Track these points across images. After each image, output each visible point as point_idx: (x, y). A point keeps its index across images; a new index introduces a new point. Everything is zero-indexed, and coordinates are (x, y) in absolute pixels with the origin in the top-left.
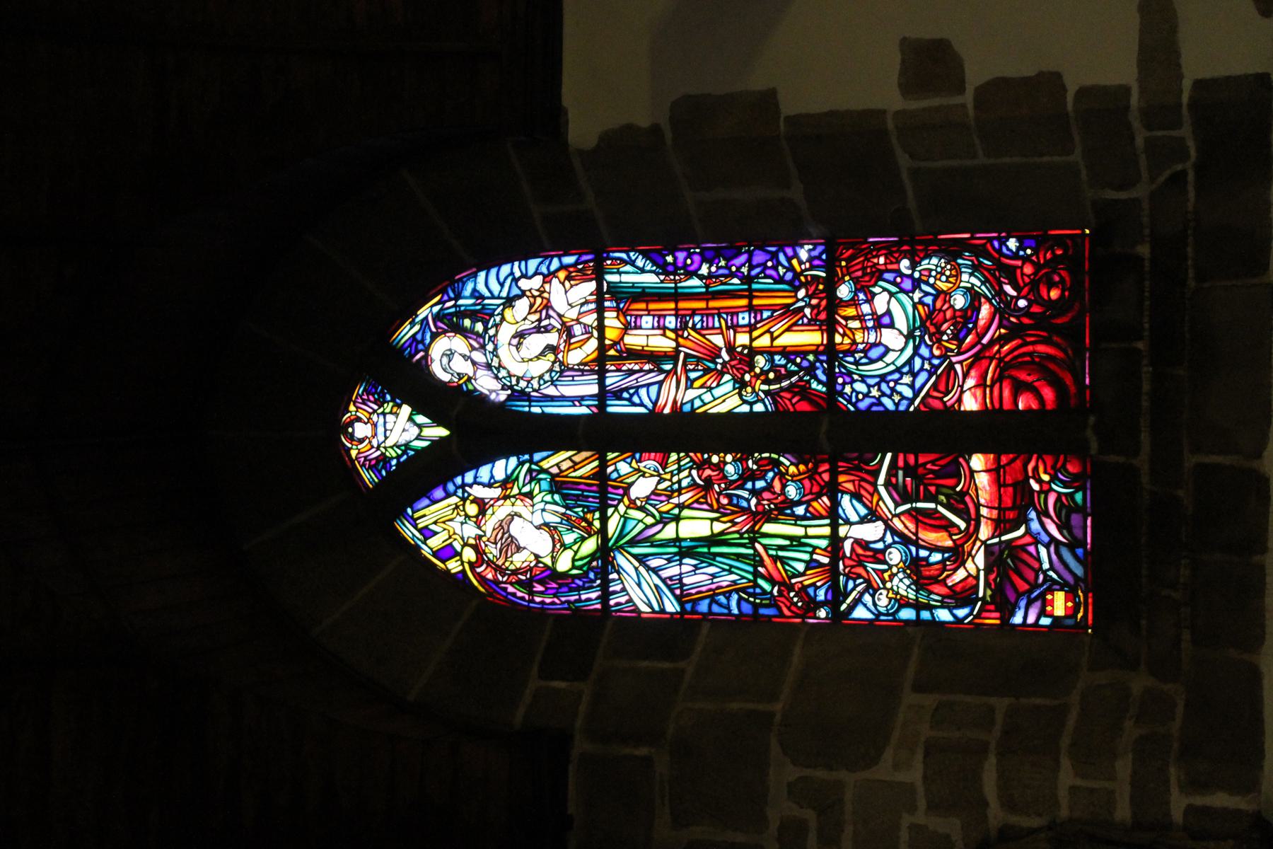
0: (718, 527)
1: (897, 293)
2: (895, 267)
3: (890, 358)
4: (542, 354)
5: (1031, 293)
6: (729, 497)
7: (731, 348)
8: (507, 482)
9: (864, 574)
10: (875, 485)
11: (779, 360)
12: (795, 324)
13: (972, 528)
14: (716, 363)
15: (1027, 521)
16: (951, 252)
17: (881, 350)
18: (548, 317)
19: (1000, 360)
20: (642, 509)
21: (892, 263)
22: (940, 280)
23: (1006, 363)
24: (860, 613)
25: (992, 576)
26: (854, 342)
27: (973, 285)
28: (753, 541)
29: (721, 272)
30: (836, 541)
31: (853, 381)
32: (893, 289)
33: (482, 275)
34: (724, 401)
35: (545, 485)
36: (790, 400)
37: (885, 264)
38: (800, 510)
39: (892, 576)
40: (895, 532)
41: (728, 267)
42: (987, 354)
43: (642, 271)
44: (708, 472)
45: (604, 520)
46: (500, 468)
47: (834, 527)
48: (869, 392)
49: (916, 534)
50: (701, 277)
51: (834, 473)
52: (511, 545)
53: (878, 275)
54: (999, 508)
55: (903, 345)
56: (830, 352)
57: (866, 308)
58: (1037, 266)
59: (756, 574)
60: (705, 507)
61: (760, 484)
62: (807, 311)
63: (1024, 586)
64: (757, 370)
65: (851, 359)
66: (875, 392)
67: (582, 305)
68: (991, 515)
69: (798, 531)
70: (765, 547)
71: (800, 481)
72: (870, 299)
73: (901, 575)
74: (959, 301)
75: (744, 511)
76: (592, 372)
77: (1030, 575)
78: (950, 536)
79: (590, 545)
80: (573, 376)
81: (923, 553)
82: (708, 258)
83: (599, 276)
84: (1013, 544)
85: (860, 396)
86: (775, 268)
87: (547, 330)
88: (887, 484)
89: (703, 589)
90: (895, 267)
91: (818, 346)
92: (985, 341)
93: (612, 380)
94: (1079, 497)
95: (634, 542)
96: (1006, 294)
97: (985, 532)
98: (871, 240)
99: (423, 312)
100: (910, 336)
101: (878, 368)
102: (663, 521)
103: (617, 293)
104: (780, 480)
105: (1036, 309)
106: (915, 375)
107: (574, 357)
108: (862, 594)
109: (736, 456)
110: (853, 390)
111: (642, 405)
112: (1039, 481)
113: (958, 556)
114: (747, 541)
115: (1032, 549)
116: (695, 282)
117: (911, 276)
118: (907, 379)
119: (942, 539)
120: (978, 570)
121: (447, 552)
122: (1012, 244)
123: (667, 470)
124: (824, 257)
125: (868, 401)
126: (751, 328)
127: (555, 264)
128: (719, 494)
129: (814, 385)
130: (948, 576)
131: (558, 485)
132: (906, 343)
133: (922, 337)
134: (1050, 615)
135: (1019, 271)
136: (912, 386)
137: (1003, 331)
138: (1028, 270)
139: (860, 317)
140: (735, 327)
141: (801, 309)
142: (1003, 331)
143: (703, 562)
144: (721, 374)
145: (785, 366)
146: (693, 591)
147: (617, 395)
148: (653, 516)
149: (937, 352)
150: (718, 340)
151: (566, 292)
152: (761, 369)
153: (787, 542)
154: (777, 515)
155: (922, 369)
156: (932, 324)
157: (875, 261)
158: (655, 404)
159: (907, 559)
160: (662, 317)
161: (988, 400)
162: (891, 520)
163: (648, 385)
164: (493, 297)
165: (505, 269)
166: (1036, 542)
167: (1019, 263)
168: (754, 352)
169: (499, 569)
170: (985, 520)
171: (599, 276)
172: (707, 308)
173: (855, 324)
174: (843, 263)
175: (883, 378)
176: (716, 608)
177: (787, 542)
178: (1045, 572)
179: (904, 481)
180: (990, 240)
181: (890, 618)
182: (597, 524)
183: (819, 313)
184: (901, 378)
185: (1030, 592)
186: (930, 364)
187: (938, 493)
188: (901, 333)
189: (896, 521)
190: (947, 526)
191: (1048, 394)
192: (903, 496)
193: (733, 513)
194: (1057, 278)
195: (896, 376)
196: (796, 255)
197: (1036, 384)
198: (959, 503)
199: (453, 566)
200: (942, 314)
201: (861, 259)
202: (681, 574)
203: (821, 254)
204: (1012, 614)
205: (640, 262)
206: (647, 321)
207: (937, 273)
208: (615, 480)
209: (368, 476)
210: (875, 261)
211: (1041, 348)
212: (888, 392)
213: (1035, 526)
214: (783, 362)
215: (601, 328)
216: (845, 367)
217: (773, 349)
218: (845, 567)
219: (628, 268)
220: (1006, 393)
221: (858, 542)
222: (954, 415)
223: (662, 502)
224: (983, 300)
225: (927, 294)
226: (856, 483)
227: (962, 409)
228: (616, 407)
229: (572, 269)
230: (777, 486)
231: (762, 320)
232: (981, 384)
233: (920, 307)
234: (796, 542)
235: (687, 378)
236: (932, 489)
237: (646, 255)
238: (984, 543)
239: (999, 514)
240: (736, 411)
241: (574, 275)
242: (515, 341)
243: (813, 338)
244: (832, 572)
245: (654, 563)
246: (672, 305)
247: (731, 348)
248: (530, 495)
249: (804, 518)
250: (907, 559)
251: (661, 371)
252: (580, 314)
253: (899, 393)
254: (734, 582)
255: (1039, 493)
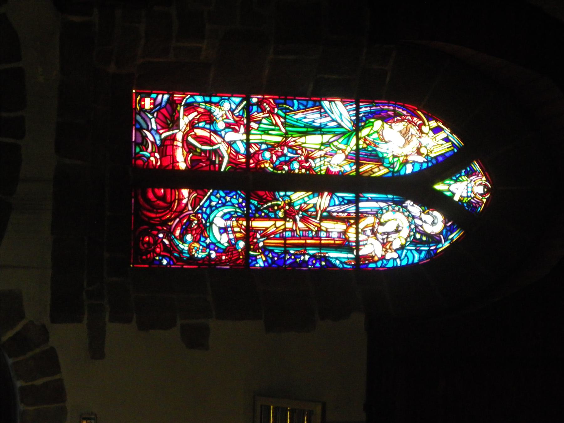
0: (303, 140)
1: (217, 243)
2: (218, 254)
3: (221, 213)
4: (386, 222)
5: (157, 240)
6: (297, 154)
7: (295, 221)
8: (406, 162)
9: (235, 117)
10: (229, 157)
11: (272, 215)
12: (264, 231)
13: (186, 137)
14: (302, 214)
15: (161, 140)
16: (192, 259)
17: (225, 217)
18: (383, 239)
19: (171, 211)
20: (339, 149)
21: (219, 256)
22: (197, 248)
23: (169, 209)
24: (237, 100)
25: (177, 115)
26: (237, 221)
27: (183, 244)
28: (286, 133)
29: (299, 256)
30: (248, 131)
31: (238, 204)
32: (218, 245)
33: (416, 260)
34: (298, 197)
35: (386, 161)
36: (267, 196)
37: (222, 256)
38: (264, 147)
39: (222, 116)
40: (220, 136)
41: (295, 258)
42: (177, 213)
43: (336, 259)
44: (307, 165)
45: (357, 145)
46: (409, 169)
47: (248, 139)
48: (230, 199)
49: (210, 135)
50: (308, 254)
51: (248, 162)
52: (405, 134)
53: (226, 251)
54: (173, 145)
55: (214, 219)
56: (248, 217)
57: (231, 236)
58: (154, 251)
59: (285, 118)
60: (309, 149)
61: (282, 159)
62: (258, 236)
63: (164, 111)
64: (282, 210)
65: (239, 214)
66: (228, 199)
67: (366, 244)
68: (177, 143)
69: (266, 137)
70: (280, 130)
71: (263, 160)
72: (229, 241)
73: (218, 117)
74: (189, 237)
75: (290, 147)
76: (362, 213)
77: (160, 115)
78: (195, 134)
79: (364, 133)
80: (371, 211)
81: (208, 126)
82: (305, 263)
83: (358, 256)
84: (167, 130)
85: (234, 197)
86: (273, 257)
87: (384, 233)
88: (223, 158)
89: (310, 112)
90: (218, 254)
91: (254, 220)
92: (178, 220)
93: (352, 209)
94: (138, 150)
95: (343, 134)
96: (168, 240)
97: (179, 136)
98: (228, 267)
99: (447, 244)
100: (212, 223)
101: (227, 209)
102: (328, 144)
103: (349, 249)
104: (273, 160)
105: (155, 232)
106: (210, 206)
107: (370, 220)
108: (236, 108)
109: (293, 172)
110: (238, 200)
111: (338, 197)
112: (155, 157)
113: (192, 125)
114: (289, 133)
115: (159, 127)
116: (312, 252)
117: (211, 249)
118: (213, 204)
119: (199, 132)
120: (183, 118)
121: (436, 130)
122: (165, 262)
123: (327, 166)
124: (250, 261)
125: (231, 195)
126: (285, 230)
127: (379, 264)
128: (301, 155)
129: (256, 203)
130: (196, 116)
131: (379, 160)
132: (213, 220)
133: (206, 222)
134: (151, 99)
135: (162, 249)
136: (211, 201)
137: (170, 224)
138: (158, 250)
139: (234, 232)
140: (292, 230)
141: (262, 237)
142: (170, 224)
143: (310, 124)
144: (301, 209)
145: (269, 212)
146: (315, 111)
147: (350, 202)
148: (333, 145)
149: (200, 215)
150: (301, 225)
151: (374, 250)
152: (280, 211)
153: (270, 132)
154: (275, 144)
155: (207, 208)
156: (202, 228)
157: (226, 258)
158: (331, 197)
159: (215, 123)
160: (328, 237)
161: (177, 193)
162: (222, 141)
163: (335, 205)
164: (411, 250)
165: (404, 263)
166: (157, 131)
167: (162, 253)
168: (284, 219)
169: (410, 122)
170: (179, 141)
171: (358, 256)
172: (306, 240)
173: (237, 229)
174: (241, 257)
175: (224, 205)
176: (305, 103)
177: (270, 132)
178: (153, 117)
179: (215, 159)
180: (174, 264)
181: (223, 98)
182: (361, 142)
183: (253, 235)
184: (216, 204)
185: (160, 109)
186: (202, 210)
187: (201, 153)
188: (216, 225)
189: (220, 141)
190: (196, 138)
191: (151, 195)
192: (217, 152)
193: (295, 146)
194: (146, 246)
195: (218, 206)
196: (264, 262)
197: (155, 199)
198: (189, 148)
199: (433, 124)
200: (197, 232)
201: (233, 259)
202: (321, 119)
203: (252, 262)
204: (168, 99)
205: (338, 262)
206: (335, 235)
207: (198, 251)
208: (352, 162)
209: (476, 167)
210: (226, 258)
211: (153, 215)
212: (222, 199)
213: (157, 137)
214: (270, 214)
215: (357, 233)
216: (241, 210)
217: (275, 219)
218: (243, 121)
219: (343, 260)
220: (169, 197)
221: (237, 131)
222: (192, 188)
223: (329, 152)
224: (178, 238)
225: (204, 242)
226: (237, 158)
227: (188, 190)
228: (350, 196)
229: (371, 261)
230: (274, 158)
231: (280, 233)
232: (180, 200)
233: (207, 235)
234: (266, 132)
235: (316, 208)
236: (203, 155)
237: (335, 266)
238: (180, 131)
239: (173, 143)
240: (292, 193)
241: (370, 258)
242: (400, 229)
243: (256, 224)
244: (250, 119)
245: (334, 124)
246: (323, 242)
247: (295, 221)
248: (394, 156)
249: (262, 143)
250: (215, 123)
251: (329, 212)
252: (367, 240)
253: (217, 197)
254: (295, 114)
255: (155, 152)
